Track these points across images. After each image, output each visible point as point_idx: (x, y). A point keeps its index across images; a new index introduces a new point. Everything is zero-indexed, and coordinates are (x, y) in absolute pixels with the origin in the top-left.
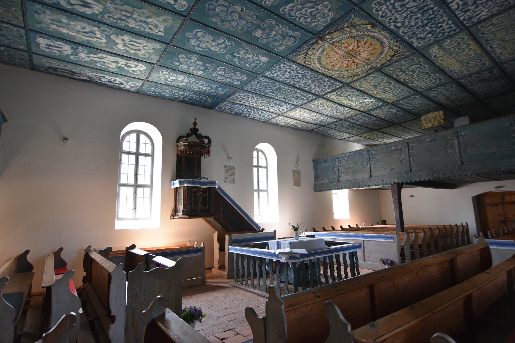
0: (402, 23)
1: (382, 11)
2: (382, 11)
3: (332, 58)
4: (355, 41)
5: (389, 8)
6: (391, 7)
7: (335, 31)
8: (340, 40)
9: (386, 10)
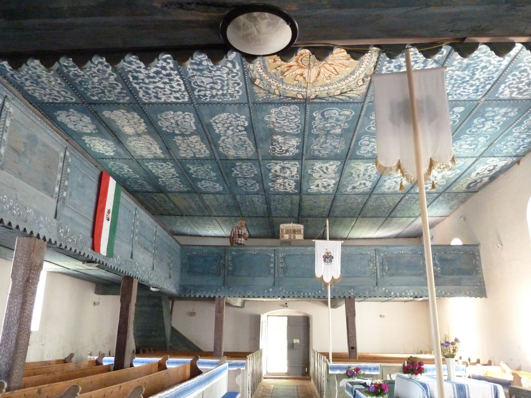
0: (225, 65)
1: (234, 88)
2: (234, 88)
3: (334, 70)
4: (285, 76)
5: (227, 87)
6: (225, 88)
7: (288, 97)
8: (295, 87)
9: (230, 88)
